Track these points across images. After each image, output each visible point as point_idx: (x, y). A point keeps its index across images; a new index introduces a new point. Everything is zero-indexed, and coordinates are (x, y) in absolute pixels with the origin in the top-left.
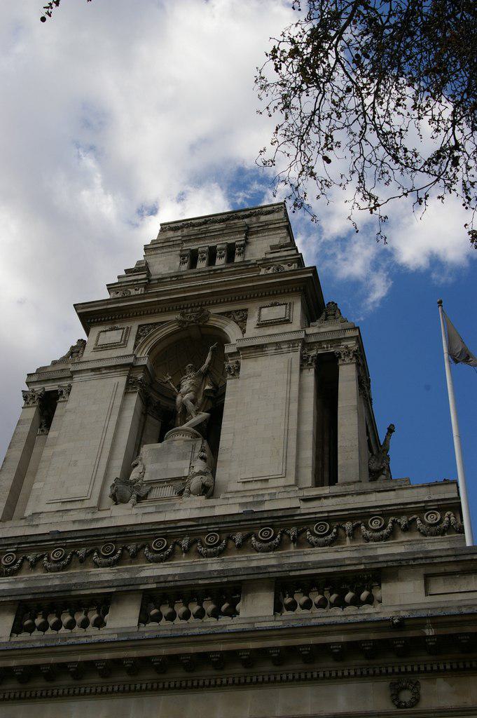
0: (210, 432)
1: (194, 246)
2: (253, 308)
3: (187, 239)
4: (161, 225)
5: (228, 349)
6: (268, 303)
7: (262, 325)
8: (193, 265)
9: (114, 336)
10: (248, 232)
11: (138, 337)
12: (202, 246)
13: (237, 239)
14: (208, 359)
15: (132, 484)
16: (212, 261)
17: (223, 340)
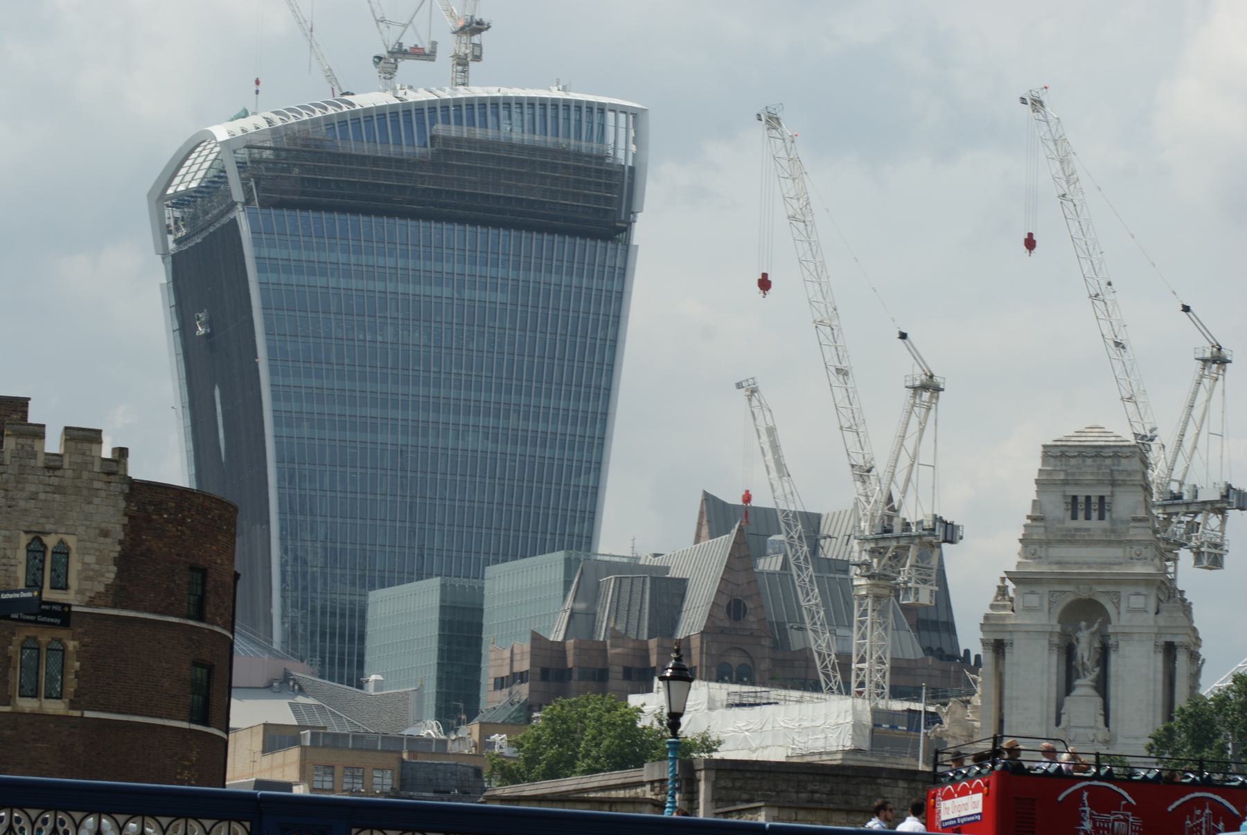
0: (1102, 685)
1: (1072, 491)
2: (1125, 591)
3: (1065, 483)
4: (1044, 446)
5: (1110, 629)
6: (1132, 590)
7: (1132, 611)
8: (1074, 517)
9: (1033, 600)
10: (1113, 483)
11: (1050, 602)
12: (1081, 493)
13: (1105, 491)
14: (1096, 626)
15: (1064, 729)
16: (1088, 517)
17: (1107, 621)
